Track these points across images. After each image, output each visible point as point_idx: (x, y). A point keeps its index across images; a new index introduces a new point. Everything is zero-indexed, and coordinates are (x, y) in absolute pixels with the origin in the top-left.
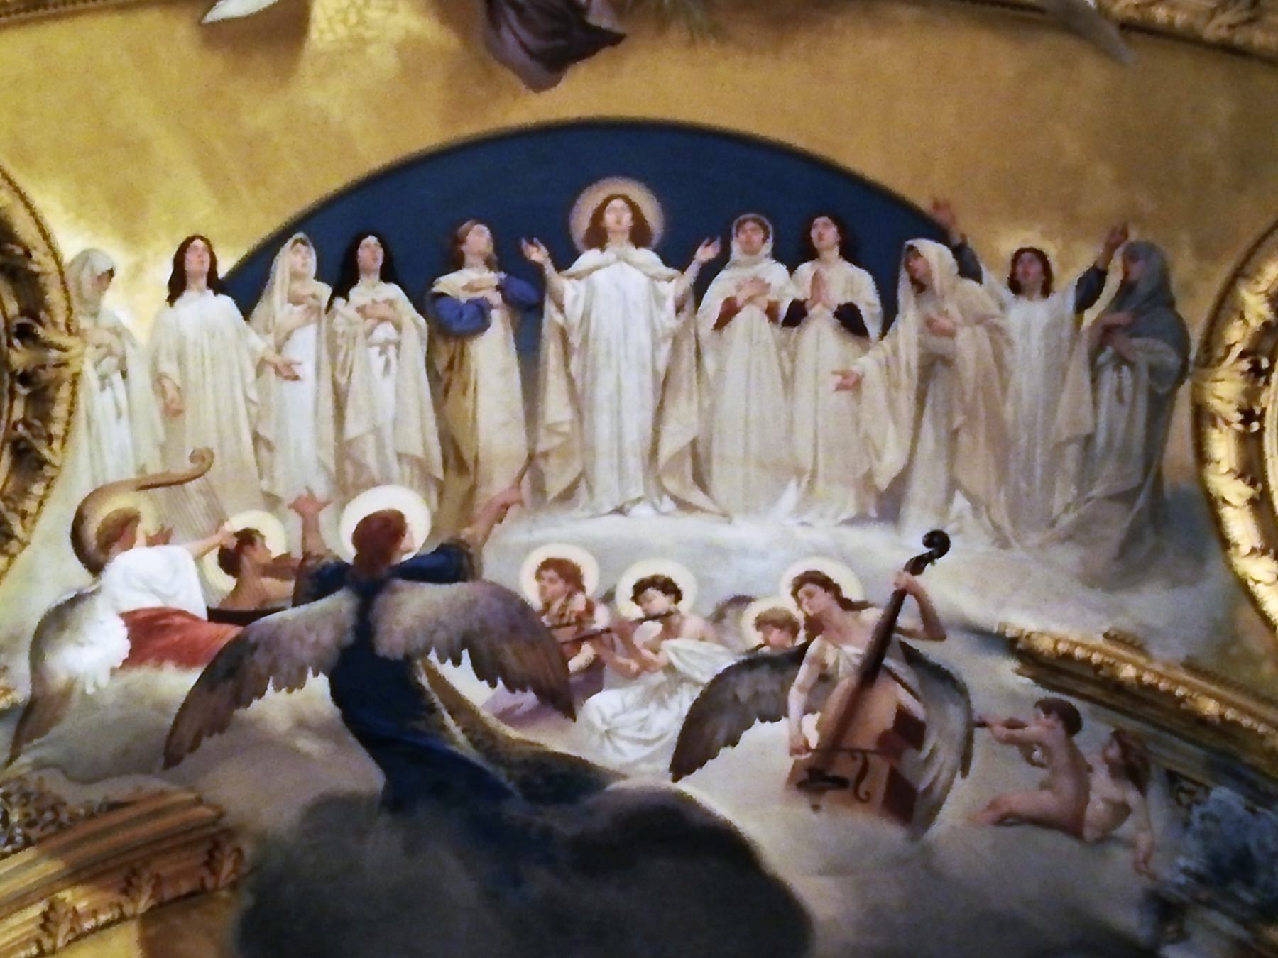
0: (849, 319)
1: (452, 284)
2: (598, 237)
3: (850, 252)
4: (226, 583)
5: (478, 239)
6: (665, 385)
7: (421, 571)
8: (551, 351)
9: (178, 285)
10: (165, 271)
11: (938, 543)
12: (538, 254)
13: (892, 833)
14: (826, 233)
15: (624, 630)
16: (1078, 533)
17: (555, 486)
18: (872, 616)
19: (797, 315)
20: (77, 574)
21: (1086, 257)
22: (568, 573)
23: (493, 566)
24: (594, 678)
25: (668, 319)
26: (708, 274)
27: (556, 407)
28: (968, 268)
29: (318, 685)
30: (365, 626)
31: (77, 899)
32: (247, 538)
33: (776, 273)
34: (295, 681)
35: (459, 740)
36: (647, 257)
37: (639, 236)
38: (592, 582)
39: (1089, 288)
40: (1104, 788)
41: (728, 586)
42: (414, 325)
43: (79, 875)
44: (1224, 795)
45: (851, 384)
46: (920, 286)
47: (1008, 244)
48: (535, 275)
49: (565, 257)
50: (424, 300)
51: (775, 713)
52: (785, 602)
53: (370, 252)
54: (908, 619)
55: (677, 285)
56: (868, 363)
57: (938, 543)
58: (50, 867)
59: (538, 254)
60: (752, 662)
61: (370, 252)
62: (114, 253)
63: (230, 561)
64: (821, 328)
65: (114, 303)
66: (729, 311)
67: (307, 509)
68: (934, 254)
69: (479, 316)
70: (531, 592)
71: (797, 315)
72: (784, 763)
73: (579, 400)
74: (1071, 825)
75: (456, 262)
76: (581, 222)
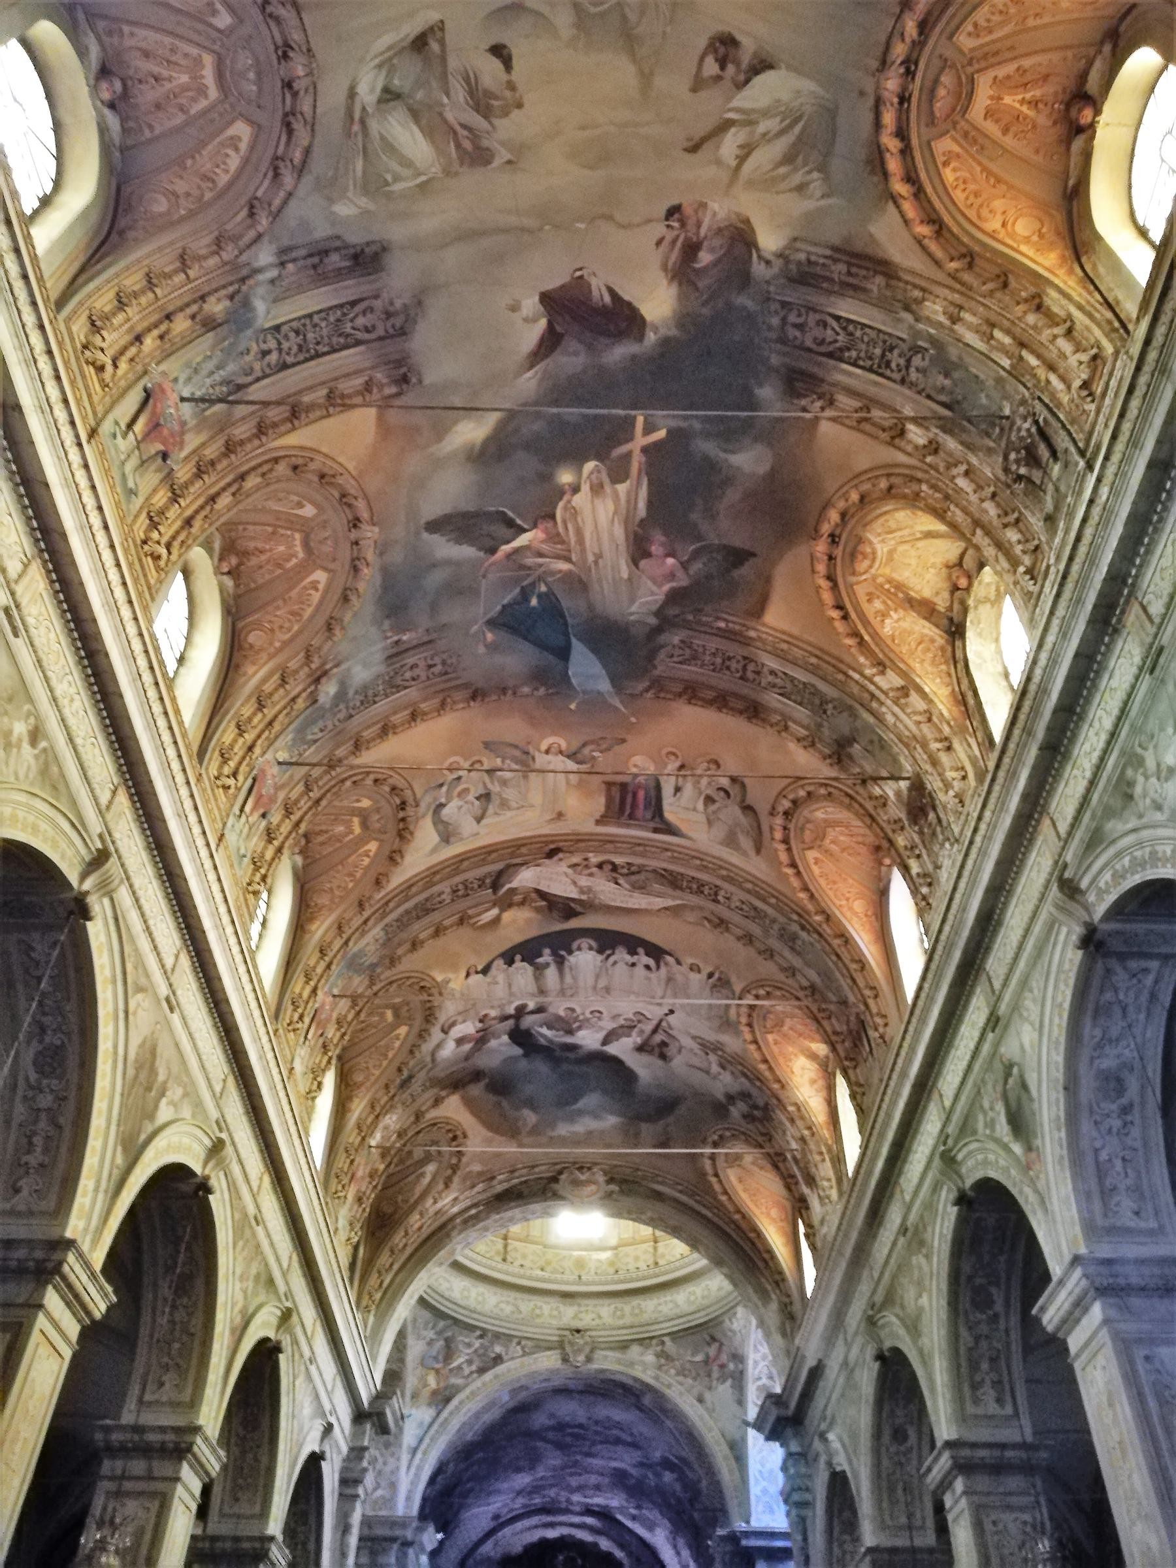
0: (648, 967)
1: (540, 960)
2: (579, 949)
3: (647, 954)
4: (480, 1025)
5: (547, 951)
6: (597, 977)
7: (532, 1012)
8: (567, 970)
9: (468, 975)
10: (464, 974)
11: (672, 1012)
12: (563, 953)
13: (660, 1062)
14: (641, 950)
15: (588, 1020)
16: (709, 1019)
17: (569, 992)
18: (655, 1022)
19: (633, 965)
20: (442, 1035)
21: (710, 969)
22: (573, 1010)
23: (551, 1010)
24: (579, 1028)
25: (599, 964)
26: (609, 956)
27: (568, 979)
28: (679, 963)
29: (505, 1038)
30: (517, 1025)
31: (443, 1093)
32: (486, 1016)
33: (628, 958)
34: (499, 1037)
35: (543, 1041)
36: (593, 953)
37: (591, 948)
38: (579, 1010)
39: (710, 975)
40: (715, 1068)
41: (615, 1012)
42: (529, 969)
43: (443, 1089)
44: (743, 1080)
45: (649, 979)
46: (666, 964)
47: (690, 961)
48: (562, 957)
49: (570, 952)
50: (531, 963)
51: (629, 1036)
52: (631, 1016)
53: (518, 957)
54: (664, 1024)
55: (600, 958)
56: (653, 975)
57: (672, 1012)
58: (435, 1090)
59: (563, 953)
60: (622, 1027)
61: (518, 957)
62: (451, 976)
63: (481, 1021)
64: (640, 971)
65: (452, 985)
66: (615, 963)
67: (501, 1007)
68: (669, 958)
69: (547, 965)
70: (562, 1013)
71: (633, 965)
72: (631, 1046)
73: (574, 978)
74: (708, 1072)
75: (541, 955)
76: (575, 945)
